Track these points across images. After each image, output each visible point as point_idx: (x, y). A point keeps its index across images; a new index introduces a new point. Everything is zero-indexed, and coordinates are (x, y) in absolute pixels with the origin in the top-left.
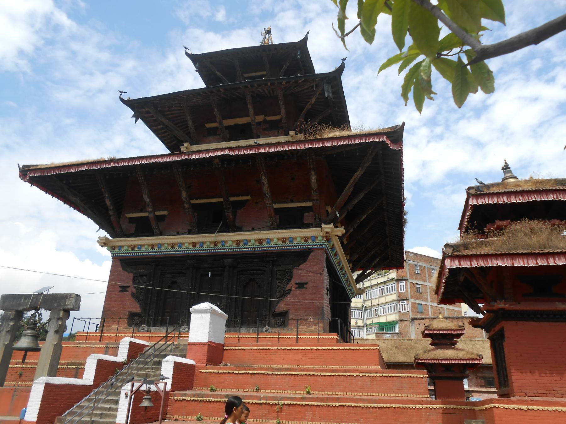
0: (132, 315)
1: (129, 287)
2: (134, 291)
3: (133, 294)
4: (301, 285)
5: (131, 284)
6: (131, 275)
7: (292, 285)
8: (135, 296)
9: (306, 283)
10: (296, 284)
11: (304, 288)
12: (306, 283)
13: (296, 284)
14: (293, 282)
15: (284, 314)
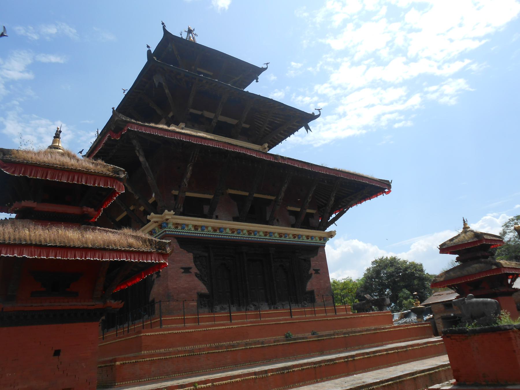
0: (201, 296)
1: (191, 268)
2: (198, 272)
3: (196, 275)
4: (317, 271)
5: (192, 265)
6: (191, 255)
7: (311, 271)
8: (199, 276)
9: (319, 270)
10: (314, 270)
11: (319, 273)
12: (319, 270)
13: (314, 270)
14: (312, 269)
15: (312, 293)
